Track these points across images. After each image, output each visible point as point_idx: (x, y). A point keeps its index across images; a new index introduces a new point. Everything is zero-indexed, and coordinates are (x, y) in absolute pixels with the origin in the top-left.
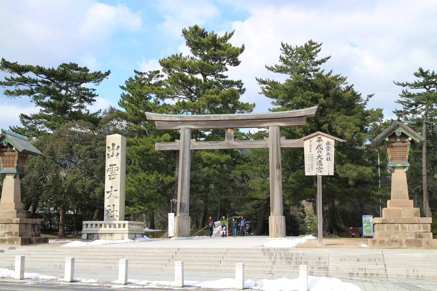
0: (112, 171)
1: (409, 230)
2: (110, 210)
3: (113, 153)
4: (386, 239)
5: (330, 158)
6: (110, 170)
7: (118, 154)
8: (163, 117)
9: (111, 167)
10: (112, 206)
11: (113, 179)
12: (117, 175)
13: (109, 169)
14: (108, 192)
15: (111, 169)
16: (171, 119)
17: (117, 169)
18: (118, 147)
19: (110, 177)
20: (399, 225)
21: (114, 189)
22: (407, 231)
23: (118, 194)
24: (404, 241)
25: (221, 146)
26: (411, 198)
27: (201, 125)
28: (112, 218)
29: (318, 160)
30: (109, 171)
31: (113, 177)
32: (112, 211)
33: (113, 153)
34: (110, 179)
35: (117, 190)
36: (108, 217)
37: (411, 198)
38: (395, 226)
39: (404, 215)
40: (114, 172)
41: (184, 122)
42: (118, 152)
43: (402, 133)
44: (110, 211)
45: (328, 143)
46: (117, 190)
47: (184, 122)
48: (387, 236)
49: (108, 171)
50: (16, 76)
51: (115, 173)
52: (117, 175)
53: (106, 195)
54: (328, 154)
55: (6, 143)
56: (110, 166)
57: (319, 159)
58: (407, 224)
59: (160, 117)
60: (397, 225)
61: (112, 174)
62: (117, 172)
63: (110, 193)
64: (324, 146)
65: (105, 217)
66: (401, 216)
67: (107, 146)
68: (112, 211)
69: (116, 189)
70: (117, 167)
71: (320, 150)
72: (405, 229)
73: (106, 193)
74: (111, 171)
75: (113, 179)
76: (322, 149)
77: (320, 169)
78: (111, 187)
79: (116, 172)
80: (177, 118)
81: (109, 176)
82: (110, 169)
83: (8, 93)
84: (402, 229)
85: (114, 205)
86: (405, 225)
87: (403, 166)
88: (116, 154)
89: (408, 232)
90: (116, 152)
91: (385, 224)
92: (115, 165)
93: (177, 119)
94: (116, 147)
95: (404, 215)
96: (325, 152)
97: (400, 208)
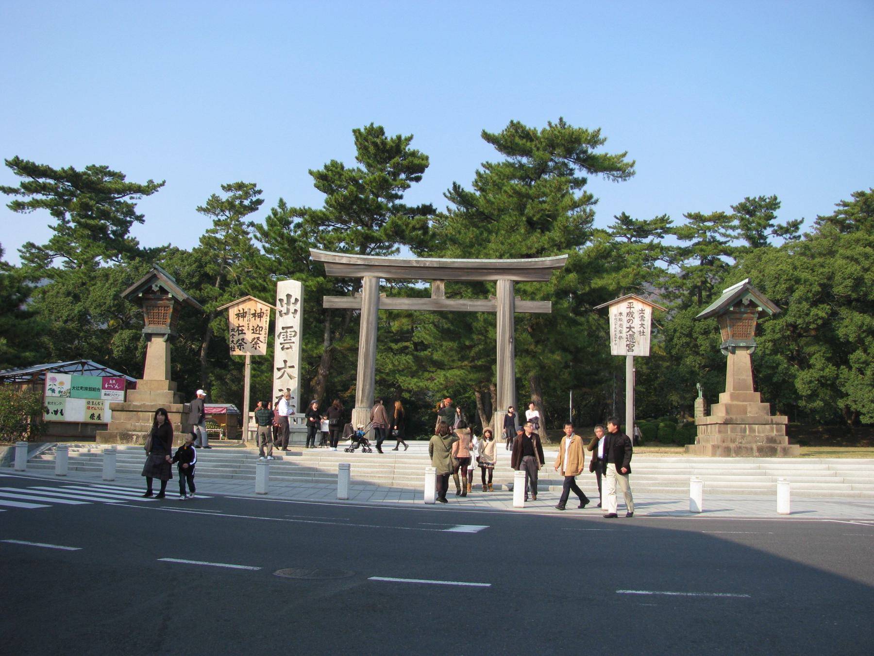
0: (287, 337)
1: (759, 432)
3: (288, 310)
4: (732, 446)
5: (643, 332)
7: (296, 311)
8: (337, 258)
9: (285, 331)
11: (288, 348)
12: (294, 343)
13: (281, 333)
14: (279, 369)
15: (285, 334)
16: (350, 261)
17: (293, 333)
18: (296, 300)
19: (282, 346)
20: (747, 426)
21: (288, 364)
22: (757, 434)
23: (295, 372)
24: (755, 447)
25: (425, 306)
26: (756, 390)
27: (396, 273)
29: (628, 334)
30: (281, 336)
31: (287, 346)
33: (288, 310)
34: (283, 349)
35: (293, 367)
37: (756, 390)
38: (741, 428)
39: (750, 412)
40: (289, 338)
41: (369, 267)
42: (295, 308)
43: (751, 301)
45: (642, 311)
46: (293, 367)
47: (369, 267)
48: (733, 441)
49: (279, 336)
50: (28, 180)
51: (291, 340)
52: (294, 343)
53: (276, 374)
54: (642, 325)
55: (156, 286)
56: (283, 328)
57: (631, 333)
58: (757, 424)
59: (334, 257)
60: (743, 426)
61: (286, 342)
62: (293, 339)
63: (283, 371)
64: (637, 316)
66: (746, 413)
67: (278, 298)
70: (295, 331)
71: (632, 318)
72: (754, 431)
73: (275, 370)
75: (288, 348)
76: (634, 318)
77: (630, 347)
78: (285, 362)
79: (292, 338)
80: (359, 261)
81: (281, 344)
82: (283, 334)
83: (18, 206)
84: (750, 431)
86: (754, 426)
87: (748, 345)
88: (292, 310)
89: (758, 436)
90: (292, 308)
91: (729, 425)
92: (292, 327)
93: (359, 262)
94: (293, 300)
95: (750, 412)
96: (636, 323)
97: (746, 403)
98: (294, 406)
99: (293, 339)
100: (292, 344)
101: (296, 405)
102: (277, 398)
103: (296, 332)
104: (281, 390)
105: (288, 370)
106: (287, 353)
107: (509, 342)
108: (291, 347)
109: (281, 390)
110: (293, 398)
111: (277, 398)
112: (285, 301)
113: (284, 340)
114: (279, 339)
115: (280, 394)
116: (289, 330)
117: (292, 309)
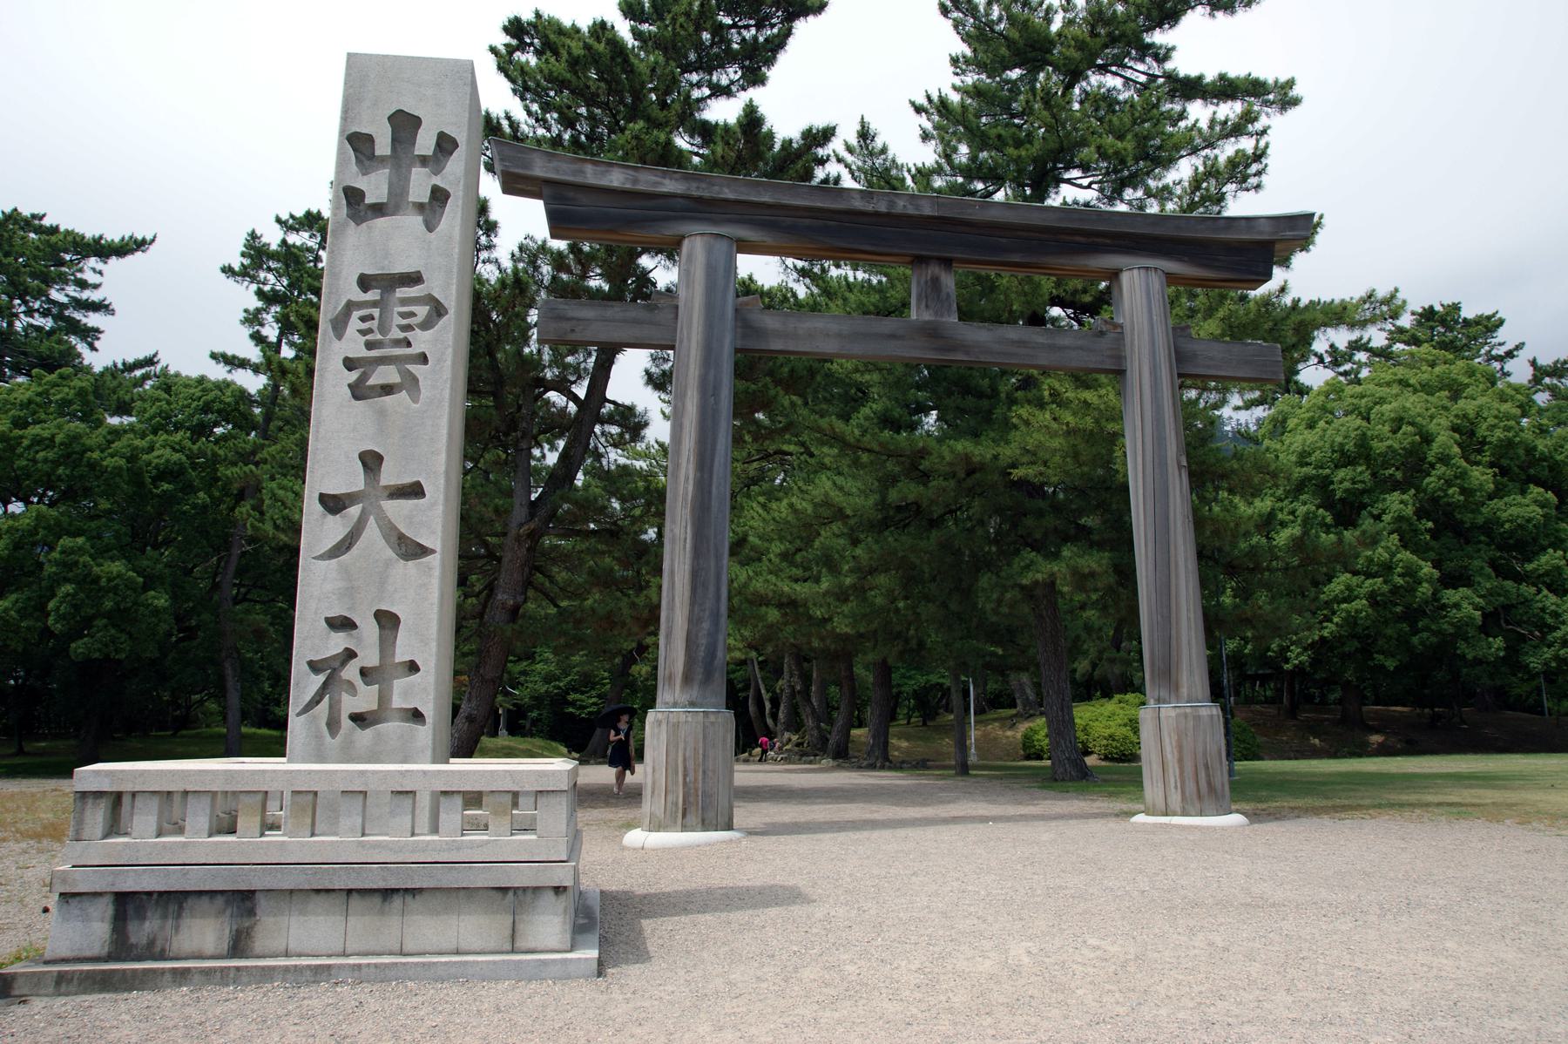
0: (383, 329)
2: (350, 654)
6: (363, 319)
9: (373, 295)
10: (369, 629)
11: (388, 390)
12: (423, 358)
13: (351, 306)
14: (334, 504)
15: (376, 312)
17: (422, 311)
19: (354, 376)
21: (390, 475)
28: (365, 736)
30: (354, 323)
31: (386, 375)
32: (364, 672)
34: (359, 391)
35: (415, 491)
36: (333, 725)
40: (396, 334)
42: (437, 181)
44: (351, 672)
46: (415, 491)
49: (339, 326)
51: (409, 344)
52: (423, 358)
56: (365, 282)
62: (422, 341)
63: (354, 511)
65: (297, 727)
68: (364, 672)
69: (407, 479)
73: (311, 508)
74: (374, 324)
75: (388, 390)
78: (372, 462)
80: (667, 182)
81: (350, 364)
82: (356, 314)
85: (388, 621)
92: (414, 279)
94: (425, 143)
98: (417, 716)
99: (422, 341)
100: (415, 369)
101: (428, 710)
102: (315, 667)
103: (438, 310)
104: (342, 624)
105: (397, 510)
106: (382, 413)
107: (1180, 467)
108: (411, 383)
109: (342, 624)
110: (413, 667)
111: (315, 667)
112: (383, 147)
113: (370, 345)
114: (339, 336)
115: (338, 642)
116: (403, 292)
117: (420, 184)
